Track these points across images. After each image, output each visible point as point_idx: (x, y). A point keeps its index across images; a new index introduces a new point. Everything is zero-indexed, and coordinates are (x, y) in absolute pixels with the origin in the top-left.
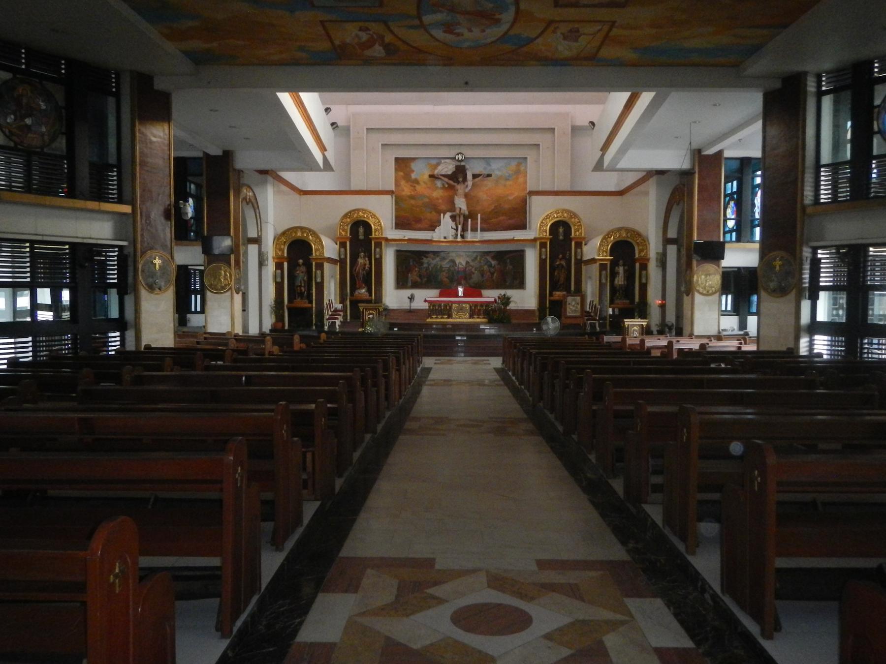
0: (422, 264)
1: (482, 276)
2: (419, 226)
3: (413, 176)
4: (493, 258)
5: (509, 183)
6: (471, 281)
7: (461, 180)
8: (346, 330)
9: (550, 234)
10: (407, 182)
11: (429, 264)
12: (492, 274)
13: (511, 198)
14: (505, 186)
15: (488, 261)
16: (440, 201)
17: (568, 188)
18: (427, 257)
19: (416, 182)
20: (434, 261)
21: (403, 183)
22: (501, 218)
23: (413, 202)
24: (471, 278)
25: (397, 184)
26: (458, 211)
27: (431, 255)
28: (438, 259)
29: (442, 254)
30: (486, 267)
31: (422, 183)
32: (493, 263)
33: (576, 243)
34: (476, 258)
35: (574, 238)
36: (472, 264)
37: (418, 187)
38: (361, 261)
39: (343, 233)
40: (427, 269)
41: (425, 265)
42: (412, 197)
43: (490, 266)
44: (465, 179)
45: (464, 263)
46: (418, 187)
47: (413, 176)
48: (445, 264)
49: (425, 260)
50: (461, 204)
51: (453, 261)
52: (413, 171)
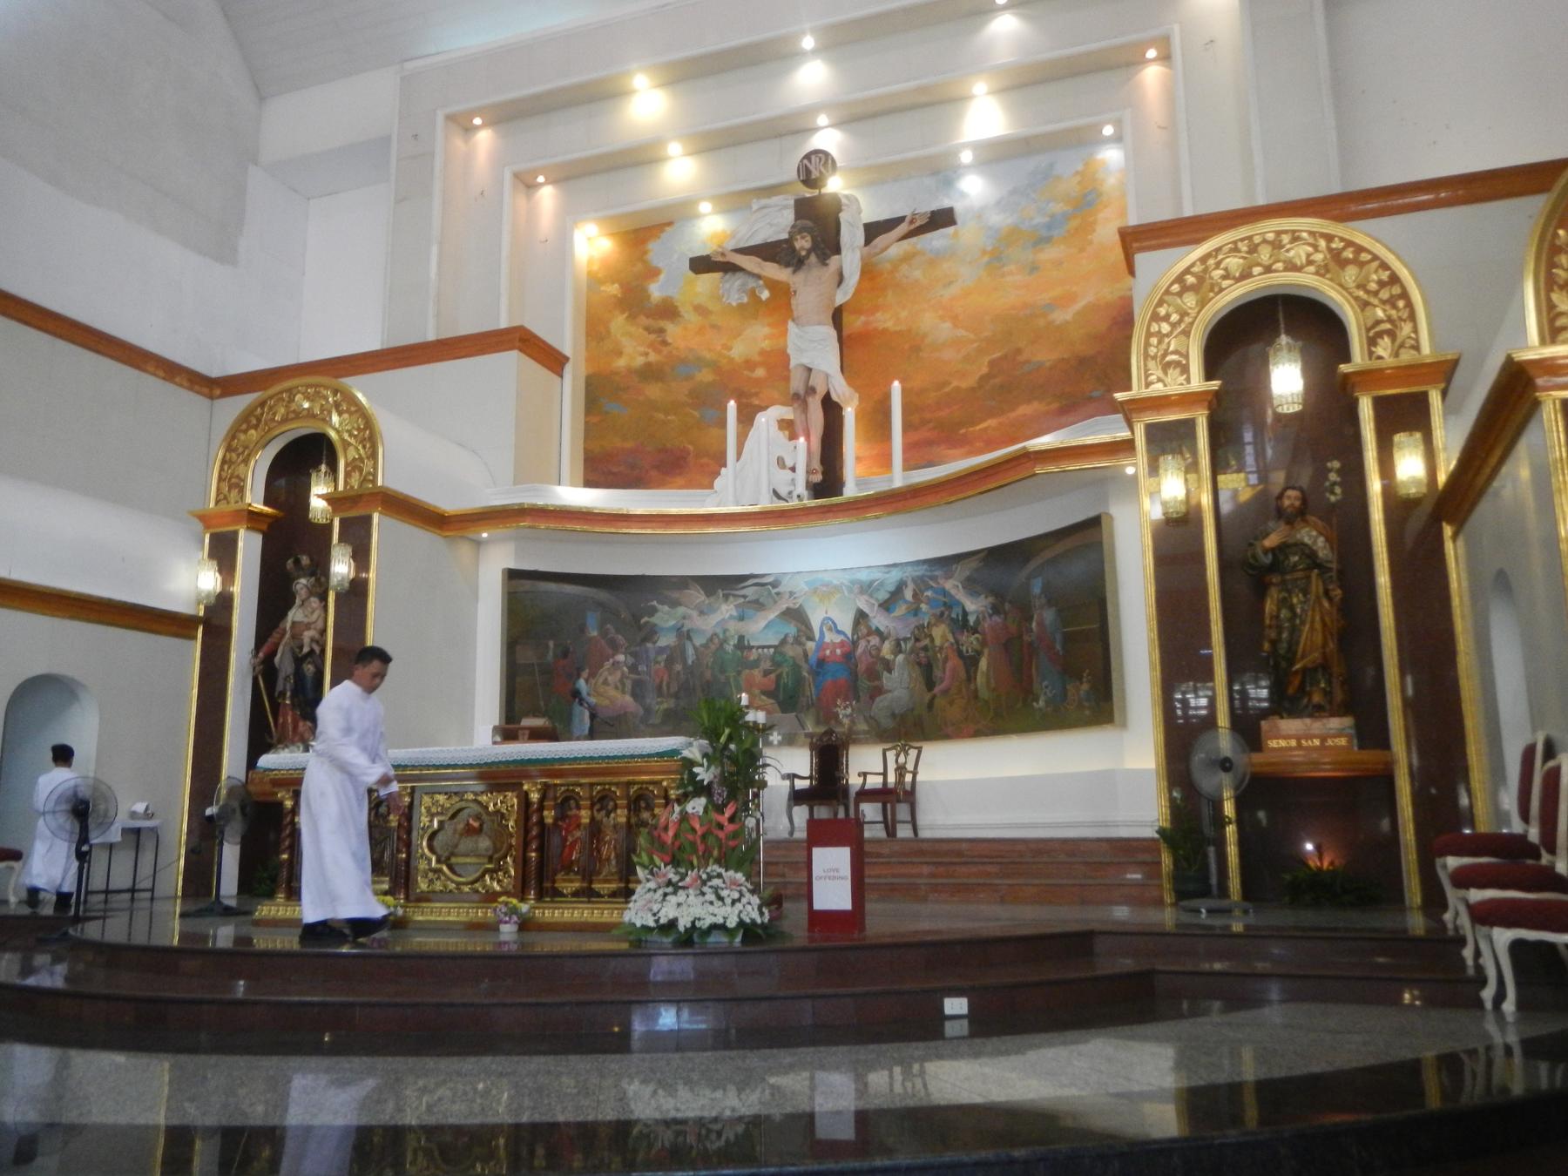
0: (651, 633)
1: (927, 671)
2: (680, 480)
3: (656, 291)
4: (971, 585)
5: (1050, 253)
6: (881, 702)
7: (803, 244)
8: (240, 948)
9: (1209, 375)
10: (632, 317)
11: (684, 635)
12: (971, 662)
13: (1061, 316)
14: (1034, 268)
15: (949, 604)
16: (760, 372)
17: (1333, 186)
18: (675, 604)
19: (668, 311)
20: (717, 619)
21: (619, 323)
22: (1024, 410)
23: (654, 391)
24: (878, 691)
25: (595, 330)
26: (797, 384)
27: (698, 596)
28: (727, 610)
29: (750, 592)
30: (940, 633)
31: (690, 316)
32: (973, 606)
33: (1380, 404)
34: (897, 593)
35: (1369, 377)
36: (879, 621)
37: (673, 331)
38: (295, 615)
39: (234, 493)
40: (675, 654)
41: (666, 640)
42: (649, 373)
43: (961, 624)
44: (828, 244)
45: (846, 623)
46: (673, 331)
47: (656, 291)
48: (763, 630)
49: (665, 618)
50: (815, 350)
51: (796, 615)
52: (654, 273)
